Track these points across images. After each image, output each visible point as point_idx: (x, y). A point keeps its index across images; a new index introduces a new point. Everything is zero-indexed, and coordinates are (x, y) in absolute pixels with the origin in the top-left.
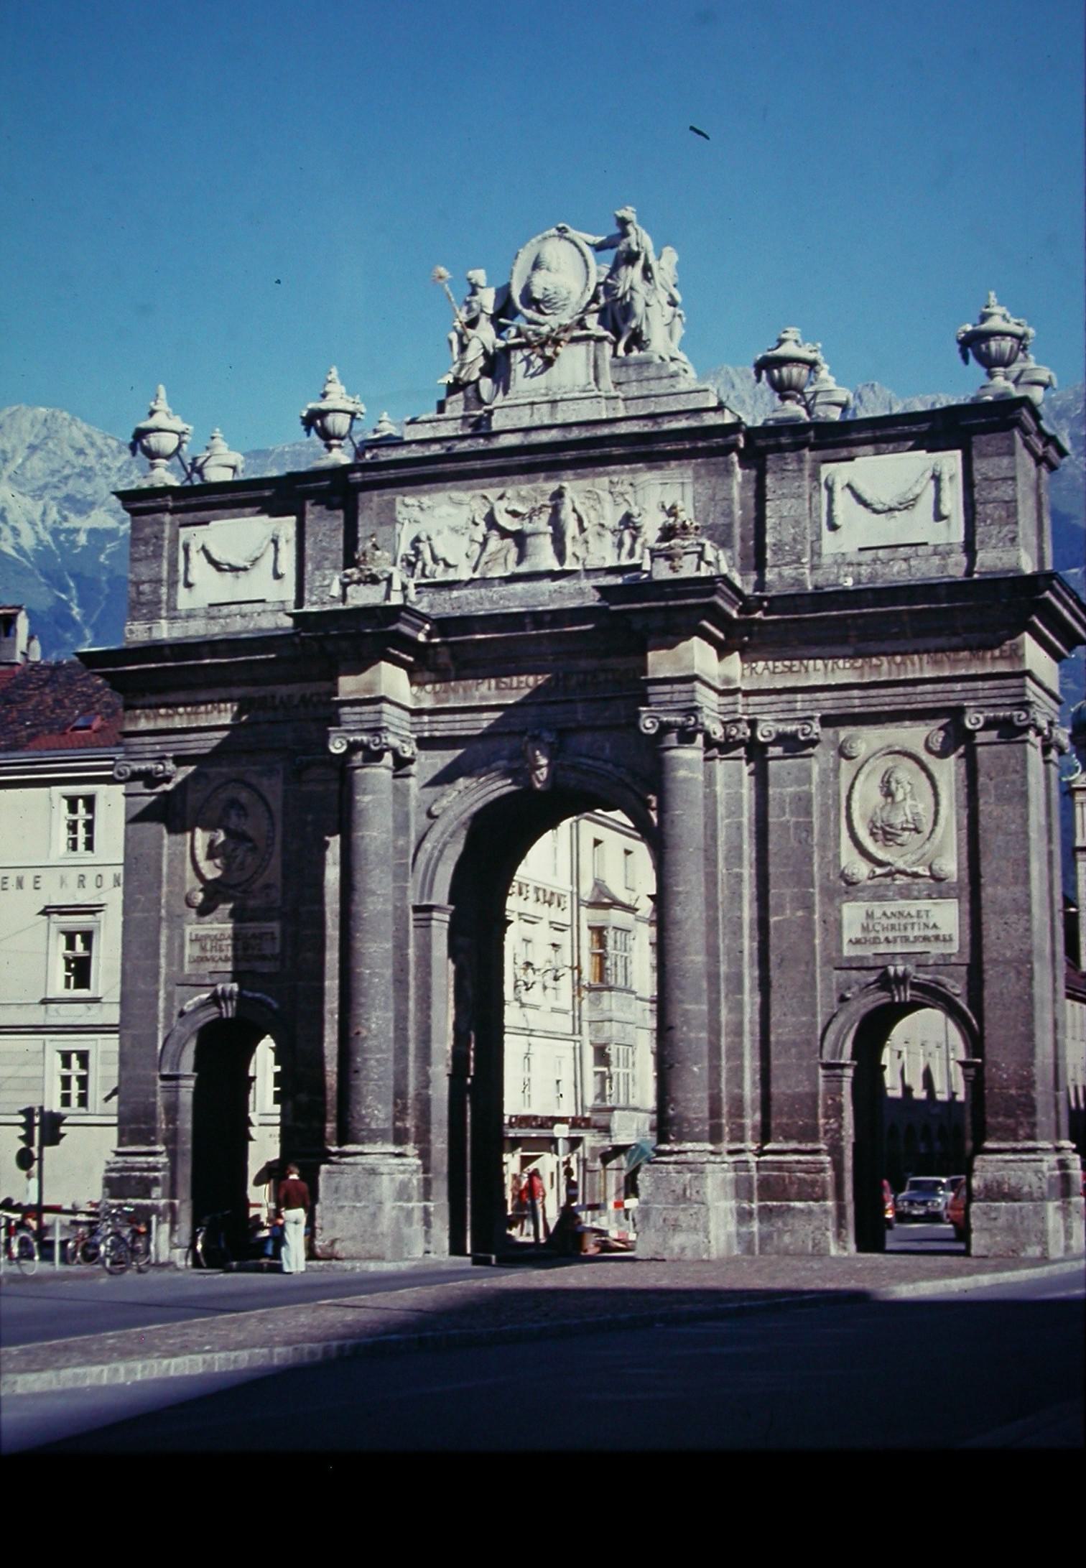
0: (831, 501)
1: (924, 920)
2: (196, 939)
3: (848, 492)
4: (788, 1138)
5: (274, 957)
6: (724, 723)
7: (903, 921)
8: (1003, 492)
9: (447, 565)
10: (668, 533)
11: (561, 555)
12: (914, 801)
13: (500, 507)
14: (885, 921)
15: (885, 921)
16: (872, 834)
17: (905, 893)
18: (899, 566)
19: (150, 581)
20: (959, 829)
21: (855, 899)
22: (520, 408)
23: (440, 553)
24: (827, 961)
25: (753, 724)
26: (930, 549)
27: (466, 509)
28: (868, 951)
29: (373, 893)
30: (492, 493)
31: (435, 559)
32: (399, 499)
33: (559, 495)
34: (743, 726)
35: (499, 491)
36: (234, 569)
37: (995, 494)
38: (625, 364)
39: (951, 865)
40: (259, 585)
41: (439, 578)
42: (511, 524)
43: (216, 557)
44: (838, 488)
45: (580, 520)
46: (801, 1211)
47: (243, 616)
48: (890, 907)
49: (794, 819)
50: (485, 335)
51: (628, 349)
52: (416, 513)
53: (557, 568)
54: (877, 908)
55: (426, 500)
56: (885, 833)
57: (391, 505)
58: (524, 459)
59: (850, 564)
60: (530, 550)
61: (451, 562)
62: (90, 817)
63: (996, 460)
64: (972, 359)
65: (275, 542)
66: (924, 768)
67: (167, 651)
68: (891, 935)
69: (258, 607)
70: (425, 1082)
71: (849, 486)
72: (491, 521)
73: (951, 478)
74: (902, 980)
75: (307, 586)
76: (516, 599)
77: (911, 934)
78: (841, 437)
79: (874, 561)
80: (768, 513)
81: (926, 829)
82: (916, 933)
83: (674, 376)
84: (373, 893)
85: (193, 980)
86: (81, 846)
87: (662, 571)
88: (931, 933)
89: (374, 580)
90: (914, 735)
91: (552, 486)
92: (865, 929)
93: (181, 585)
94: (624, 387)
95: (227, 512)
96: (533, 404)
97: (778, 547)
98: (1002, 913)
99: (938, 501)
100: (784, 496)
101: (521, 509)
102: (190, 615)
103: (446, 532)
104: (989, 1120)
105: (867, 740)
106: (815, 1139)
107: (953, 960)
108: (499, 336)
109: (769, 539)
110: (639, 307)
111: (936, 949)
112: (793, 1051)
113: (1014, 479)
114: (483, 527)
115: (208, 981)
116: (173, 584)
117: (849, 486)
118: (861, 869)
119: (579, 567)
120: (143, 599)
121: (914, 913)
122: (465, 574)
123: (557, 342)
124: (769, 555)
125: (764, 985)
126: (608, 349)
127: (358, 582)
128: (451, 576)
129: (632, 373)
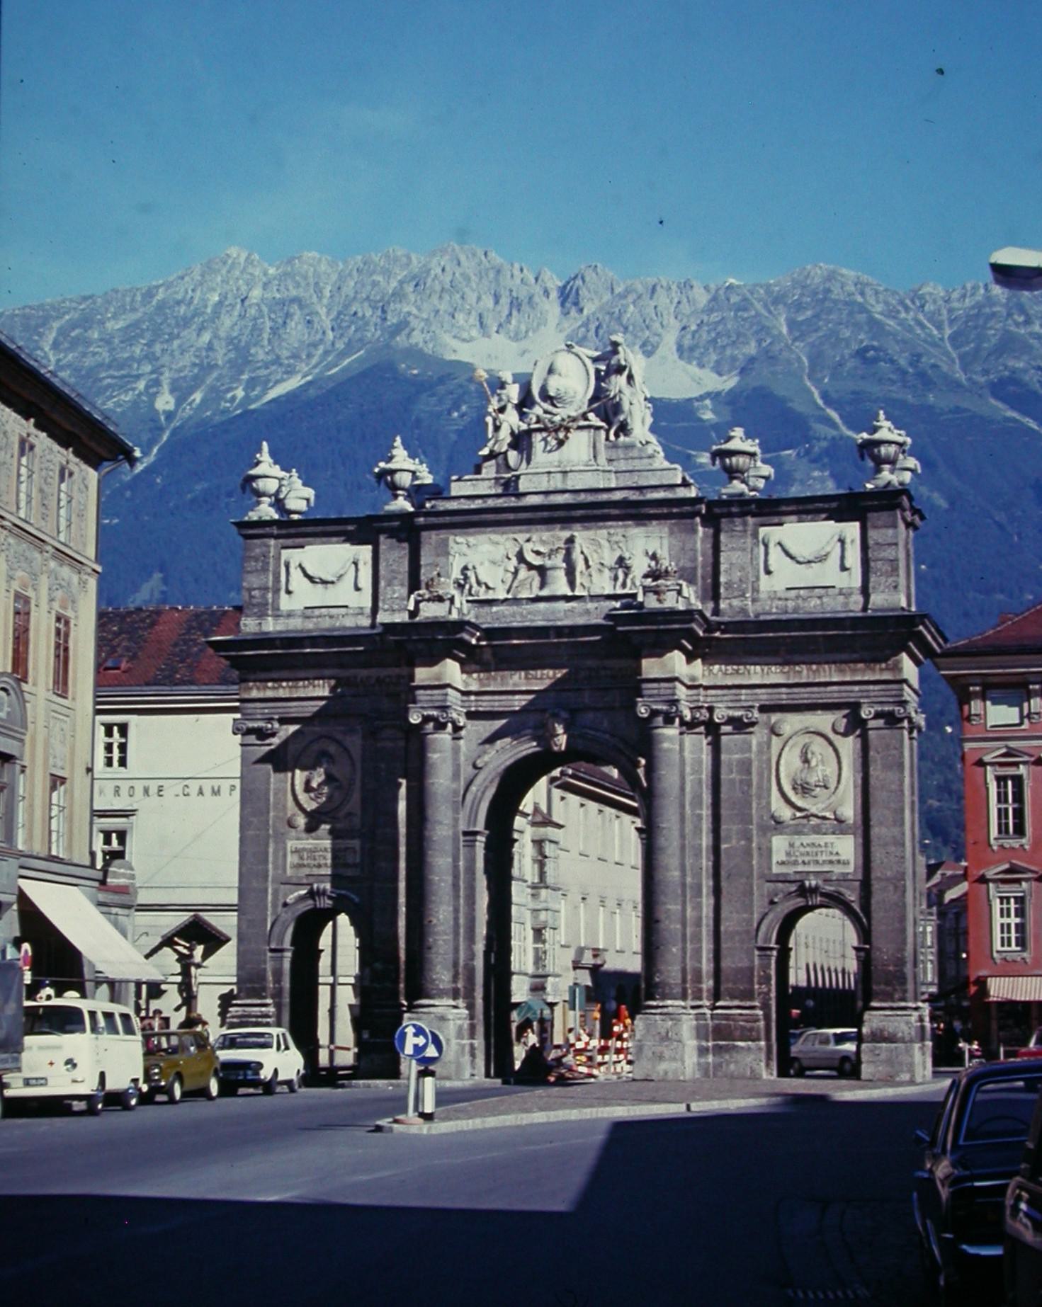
0: (767, 554)
2: (296, 851)
3: (779, 548)
4: (733, 997)
5: (355, 865)
6: (691, 709)
8: (889, 553)
9: (488, 588)
10: (654, 574)
11: (572, 584)
12: (823, 767)
13: (528, 548)
15: (802, 849)
16: (794, 789)
17: (817, 830)
18: (814, 602)
19: (259, 589)
20: (855, 787)
21: (781, 834)
22: (542, 473)
23: (483, 578)
24: (761, 876)
25: (711, 710)
26: (837, 591)
27: (501, 548)
28: (789, 870)
29: (440, 823)
30: (521, 537)
31: (479, 583)
32: (451, 538)
33: (571, 540)
34: (704, 711)
35: (527, 536)
36: (324, 582)
37: (883, 554)
38: (615, 446)
39: (849, 811)
40: (342, 594)
41: (482, 597)
42: (537, 561)
43: (310, 572)
44: (771, 545)
45: (586, 560)
46: (742, 1048)
47: (331, 617)
48: (806, 840)
49: (738, 777)
50: (511, 420)
51: (617, 435)
52: (464, 548)
53: (570, 594)
54: (798, 840)
55: (471, 540)
56: (803, 788)
57: (445, 543)
58: (546, 514)
59: (780, 599)
60: (549, 580)
61: (491, 585)
62: (123, 740)
63: (884, 531)
64: (866, 457)
65: (356, 564)
66: (831, 743)
67: (278, 642)
68: (806, 859)
69: (343, 611)
70: (472, 956)
71: (780, 544)
72: (521, 557)
73: (852, 541)
74: (815, 890)
75: (381, 598)
76: (539, 616)
78: (770, 508)
79: (798, 597)
80: (722, 560)
81: (832, 786)
82: (824, 858)
83: (650, 457)
84: (440, 823)
85: (294, 881)
86: (115, 763)
87: (651, 603)
88: (834, 858)
89: (440, 599)
90: (823, 721)
91: (566, 534)
92: (788, 854)
93: (283, 593)
94: (615, 463)
95: (318, 540)
96: (549, 473)
97: (729, 585)
98: (886, 845)
99: (842, 558)
100: (733, 549)
101: (542, 549)
102: (290, 615)
103: (487, 564)
104: (875, 987)
105: (791, 723)
106: (751, 998)
107: (850, 877)
108: (521, 420)
109: (723, 579)
110: (626, 406)
111: (838, 869)
112: (737, 938)
113: (896, 544)
114: (514, 561)
115: (305, 881)
116: (277, 591)
117: (780, 544)
118: (786, 813)
119: (585, 593)
120: (255, 601)
122: (501, 595)
123: (567, 429)
124: (722, 590)
125: (717, 892)
126: (603, 433)
127: (428, 600)
128: (491, 595)
129: (621, 453)
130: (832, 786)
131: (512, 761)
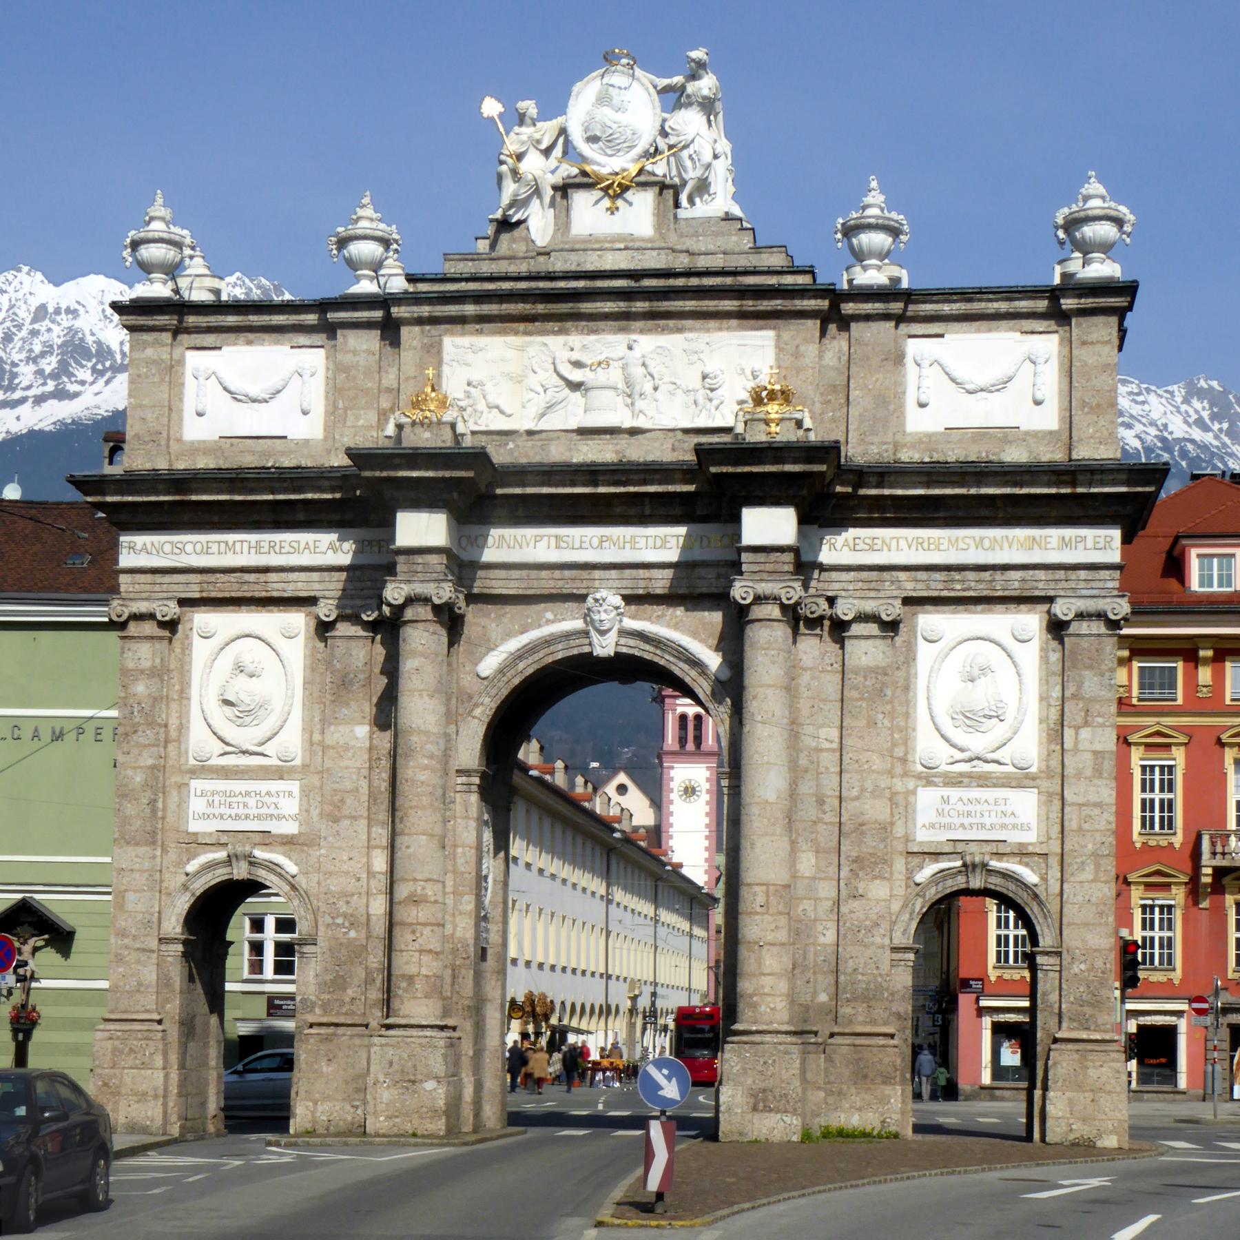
1: (1000, 809)
7: (978, 808)
14: (960, 807)
17: (984, 781)
23: (492, 399)
25: (831, 601)
28: (943, 836)
44: (925, 364)
54: (954, 793)
68: (967, 821)
77: (987, 821)
82: (993, 820)
88: (1011, 820)
92: (940, 813)
107: (1031, 849)
121: (992, 801)
130: (1010, 714)
131: (530, 671)
